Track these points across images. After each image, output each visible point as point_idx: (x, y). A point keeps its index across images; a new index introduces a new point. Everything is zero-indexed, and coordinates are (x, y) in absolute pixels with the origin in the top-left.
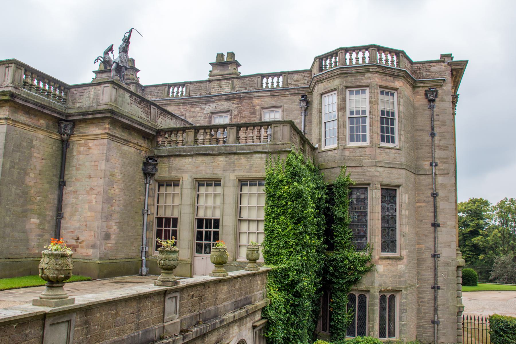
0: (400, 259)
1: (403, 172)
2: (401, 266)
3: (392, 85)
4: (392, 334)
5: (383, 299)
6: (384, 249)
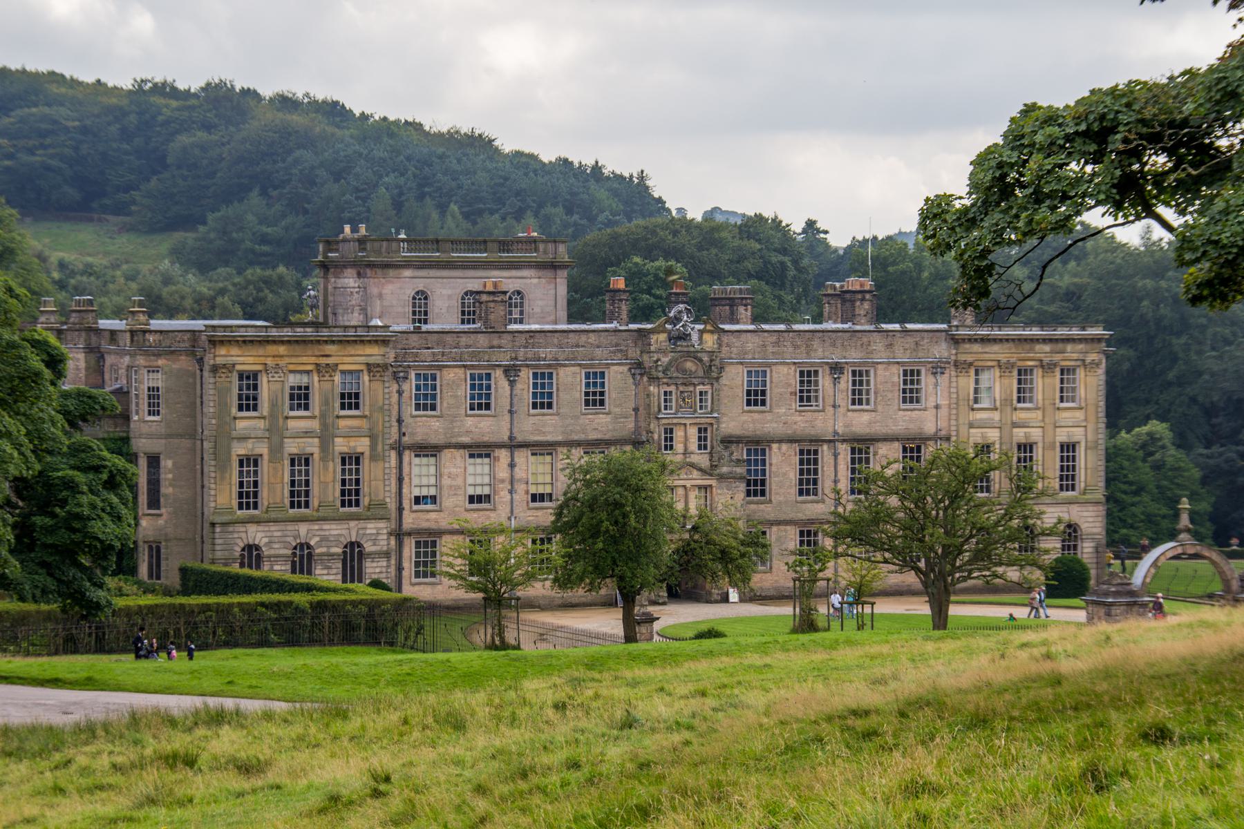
0: (160, 515)
1: (163, 441)
2: (161, 522)
3: (155, 364)
4: (158, 578)
5: (150, 548)
6: (150, 507)
